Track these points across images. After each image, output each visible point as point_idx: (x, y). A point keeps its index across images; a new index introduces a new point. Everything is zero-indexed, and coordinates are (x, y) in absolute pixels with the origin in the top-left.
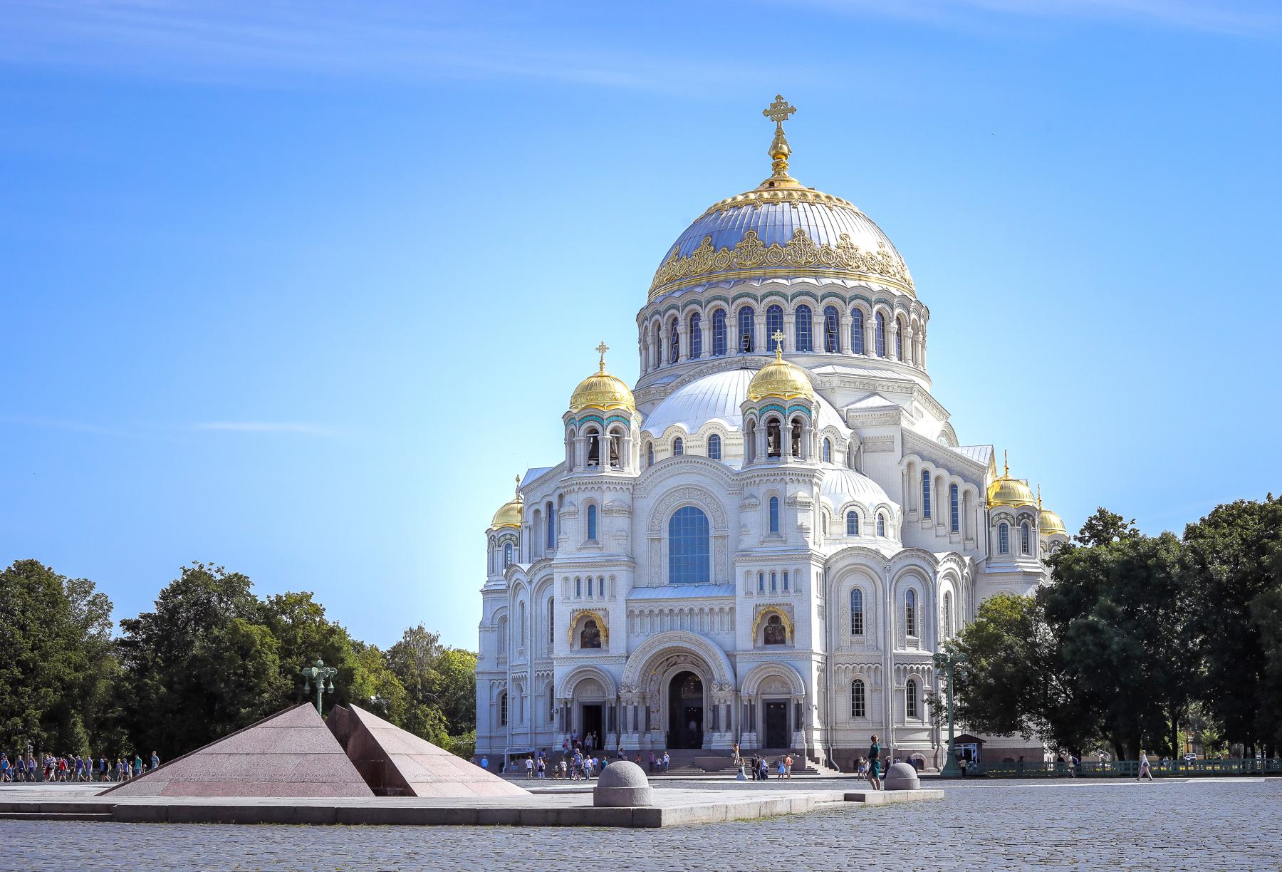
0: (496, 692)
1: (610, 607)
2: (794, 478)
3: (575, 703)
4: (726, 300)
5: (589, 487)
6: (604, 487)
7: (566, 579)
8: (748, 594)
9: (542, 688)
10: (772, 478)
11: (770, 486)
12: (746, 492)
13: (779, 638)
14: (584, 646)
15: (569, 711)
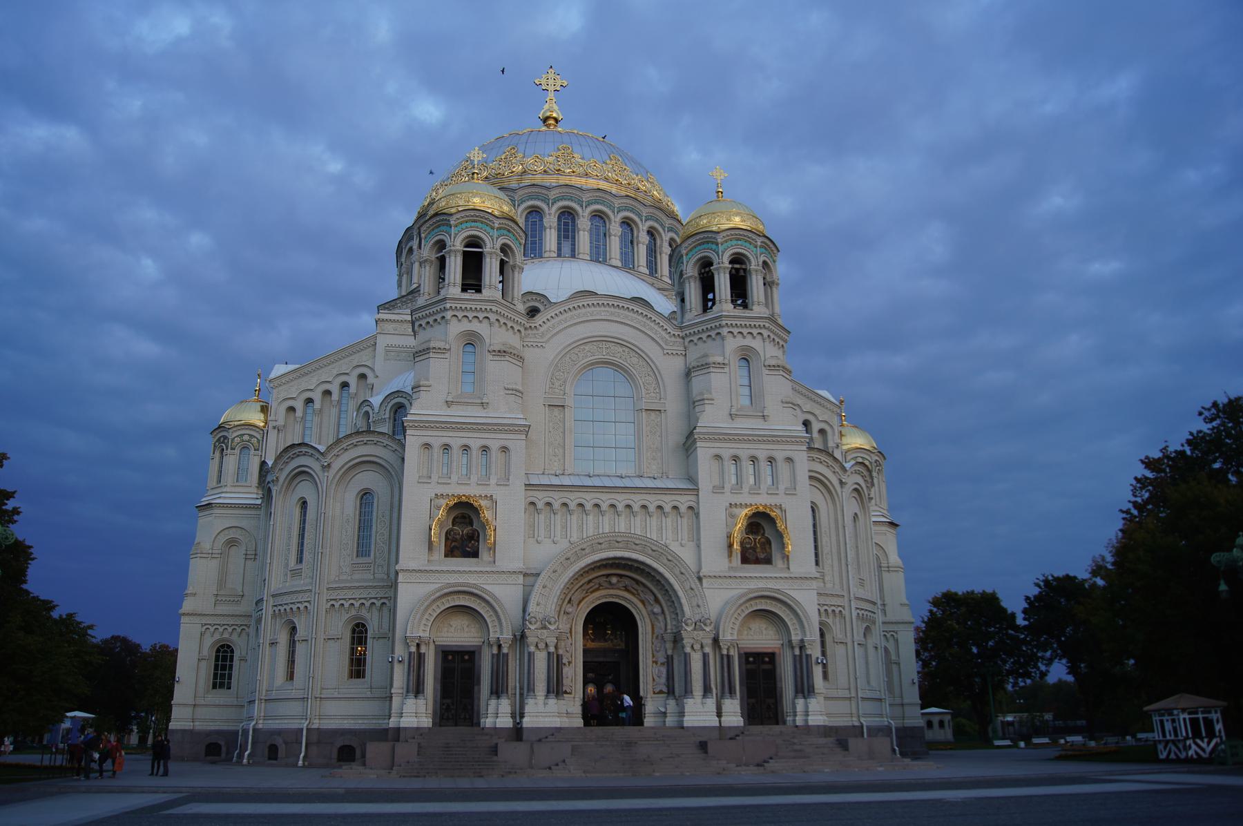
0: (209, 641)
1: (498, 493)
2: (772, 336)
3: (432, 647)
4: (546, 200)
5: (470, 315)
6: (493, 317)
7: (427, 446)
8: (718, 489)
9: (340, 627)
10: (745, 331)
11: (740, 341)
12: (694, 354)
13: (762, 556)
14: (450, 553)
15: (421, 657)
